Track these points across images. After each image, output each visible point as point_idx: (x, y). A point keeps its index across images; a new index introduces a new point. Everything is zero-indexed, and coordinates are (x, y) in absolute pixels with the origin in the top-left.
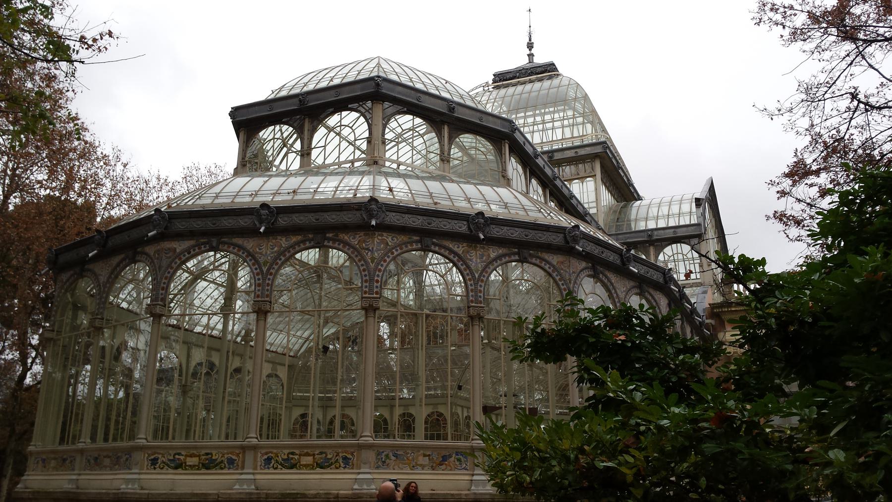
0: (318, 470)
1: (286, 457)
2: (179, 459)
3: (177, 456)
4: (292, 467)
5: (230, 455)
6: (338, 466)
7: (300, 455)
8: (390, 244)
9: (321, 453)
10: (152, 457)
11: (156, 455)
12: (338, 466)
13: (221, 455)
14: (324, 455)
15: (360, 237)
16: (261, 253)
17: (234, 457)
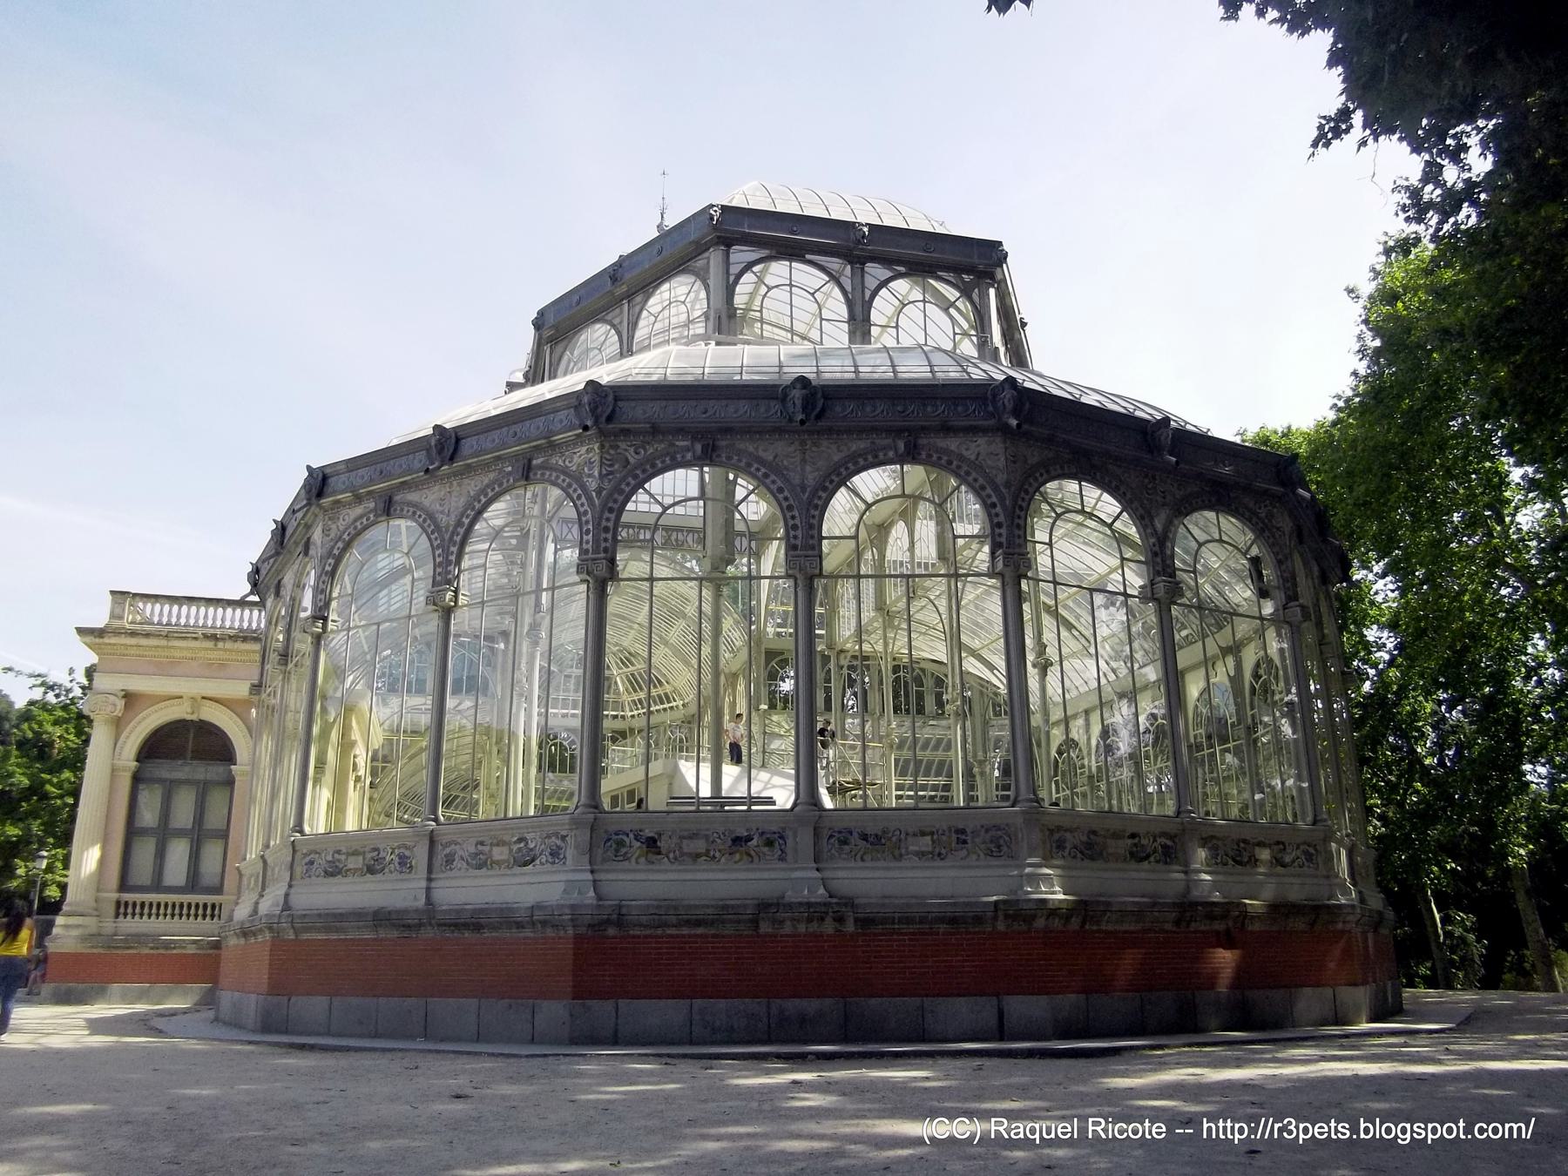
0: (517, 870)
1: (472, 849)
2: (339, 861)
3: (336, 856)
5: (402, 850)
6: (543, 860)
7: (491, 845)
8: (632, 460)
9: (520, 840)
10: (307, 859)
11: (312, 856)
12: (543, 860)
13: (390, 851)
14: (522, 845)
15: (580, 456)
16: (442, 512)
17: (407, 853)
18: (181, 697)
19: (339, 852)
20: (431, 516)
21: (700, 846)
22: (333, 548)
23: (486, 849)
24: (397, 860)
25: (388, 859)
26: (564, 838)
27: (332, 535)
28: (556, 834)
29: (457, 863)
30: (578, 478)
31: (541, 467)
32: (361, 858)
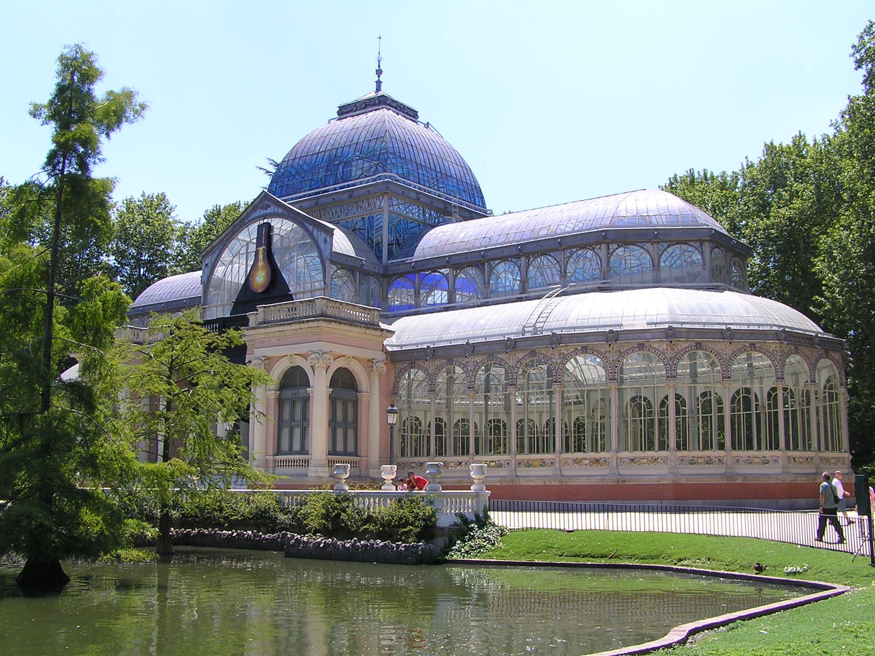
1: (746, 459)
4: (751, 463)
9: (764, 457)
18: (344, 356)
19: (694, 457)
20: (719, 354)
21: (801, 460)
22: (676, 356)
23: (751, 459)
24: (717, 460)
25: (714, 460)
26: (778, 457)
27: (676, 351)
28: (775, 456)
29: (741, 462)
30: (773, 354)
31: (759, 347)
32: (703, 459)
